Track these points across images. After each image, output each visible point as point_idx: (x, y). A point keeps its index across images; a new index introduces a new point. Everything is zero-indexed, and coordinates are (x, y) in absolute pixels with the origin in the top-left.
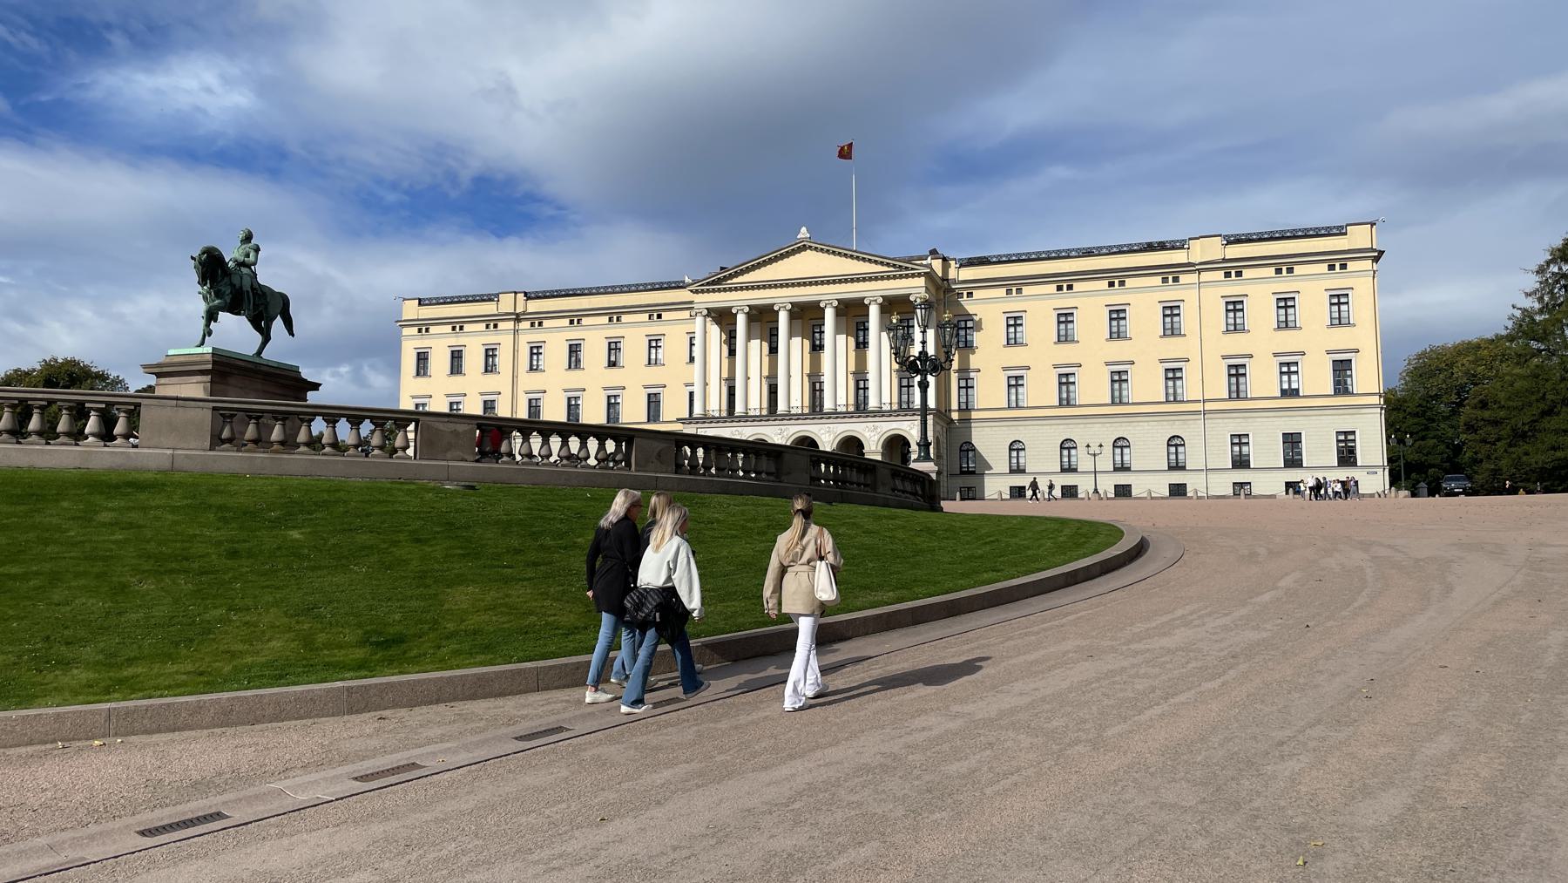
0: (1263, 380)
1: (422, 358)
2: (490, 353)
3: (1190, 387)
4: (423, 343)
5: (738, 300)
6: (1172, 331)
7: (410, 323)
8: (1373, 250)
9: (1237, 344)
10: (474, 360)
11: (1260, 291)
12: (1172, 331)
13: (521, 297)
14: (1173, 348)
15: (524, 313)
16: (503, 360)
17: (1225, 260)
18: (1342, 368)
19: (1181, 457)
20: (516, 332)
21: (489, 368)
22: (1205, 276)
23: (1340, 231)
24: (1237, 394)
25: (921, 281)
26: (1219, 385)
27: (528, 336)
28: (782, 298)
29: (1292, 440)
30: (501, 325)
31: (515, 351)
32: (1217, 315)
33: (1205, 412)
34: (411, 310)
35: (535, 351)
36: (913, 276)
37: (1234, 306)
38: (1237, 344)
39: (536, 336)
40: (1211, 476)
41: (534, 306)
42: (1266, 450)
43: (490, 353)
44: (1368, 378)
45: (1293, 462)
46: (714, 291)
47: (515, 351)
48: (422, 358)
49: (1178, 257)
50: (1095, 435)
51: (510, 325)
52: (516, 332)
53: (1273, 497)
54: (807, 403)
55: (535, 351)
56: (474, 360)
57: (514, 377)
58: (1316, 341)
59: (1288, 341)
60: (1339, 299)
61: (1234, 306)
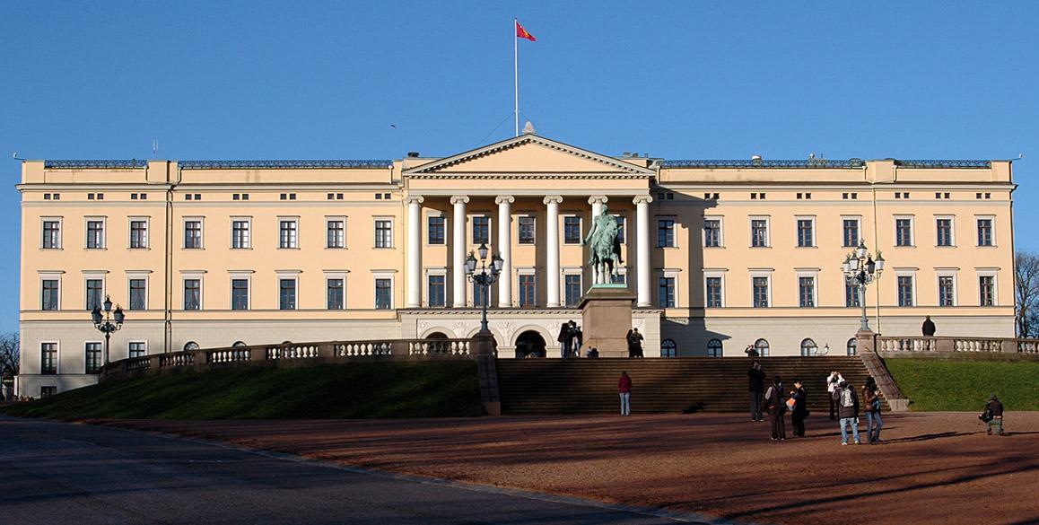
1: (49, 229)
4: (51, 210)
5: (458, 190)
7: (33, 185)
13: (174, 166)
15: (179, 184)
16: (154, 235)
17: (896, 182)
18: (986, 283)
20: (169, 204)
21: (135, 244)
22: (881, 195)
23: (986, 165)
27: (183, 211)
28: (504, 191)
30: (151, 196)
34: (32, 171)
35: (191, 227)
39: (193, 210)
41: (190, 176)
44: (1004, 292)
52: (169, 204)
54: (563, 298)
55: (191, 227)
59: (946, 256)
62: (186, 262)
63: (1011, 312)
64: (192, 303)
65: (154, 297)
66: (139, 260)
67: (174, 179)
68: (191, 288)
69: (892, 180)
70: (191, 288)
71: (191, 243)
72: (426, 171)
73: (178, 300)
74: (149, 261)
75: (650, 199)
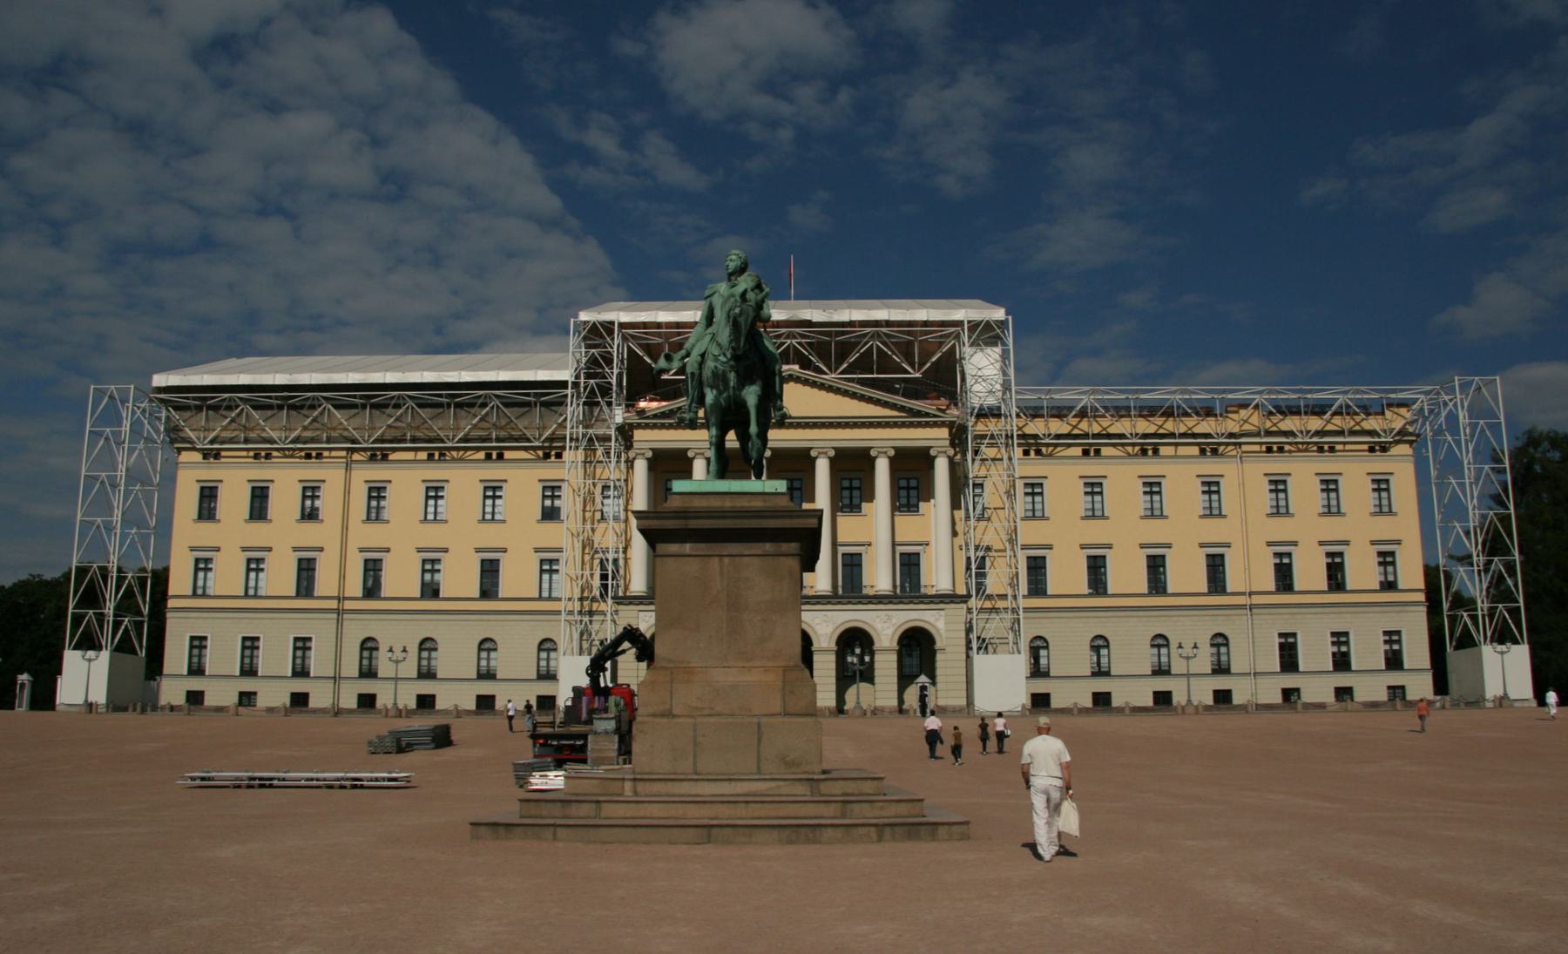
0: (1310, 572)
1: (208, 495)
2: (310, 491)
3: (1234, 578)
6: (1213, 512)
9: (1281, 529)
10: (286, 501)
11: (1303, 473)
12: (1213, 512)
14: (1214, 531)
16: (328, 503)
18: (1387, 559)
19: (1224, 658)
21: (310, 515)
25: (944, 433)
27: (365, 474)
29: (1340, 638)
31: (347, 492)
33: (1252, 607)
35: (376, 492)
36: (935, 425)
40: (1260, 680)
42: (1315, 652)
43: (310, 491)
45: (1342, 662)
46: (663, 426)
47: (347, 492)
48: (208, 495)
50: (1190, 633)
52: (348, 468)
53: (1321, 706)
55: (376, 492)
56: (286, 501)
57: (345, 527)
58: (1359, 530)
59: (1333, 529)
60: (1381, 485)
61: (1278, 485)
62: (367, 535)
63: (1421, 597)
64: (372, 590)
65: (325, 582)
66: (310, 534)
68: (373, 569)
70: (373, 569)
71: (374, 515)
72: (655, 416)
73: (355, 586)
75: (951, 452)
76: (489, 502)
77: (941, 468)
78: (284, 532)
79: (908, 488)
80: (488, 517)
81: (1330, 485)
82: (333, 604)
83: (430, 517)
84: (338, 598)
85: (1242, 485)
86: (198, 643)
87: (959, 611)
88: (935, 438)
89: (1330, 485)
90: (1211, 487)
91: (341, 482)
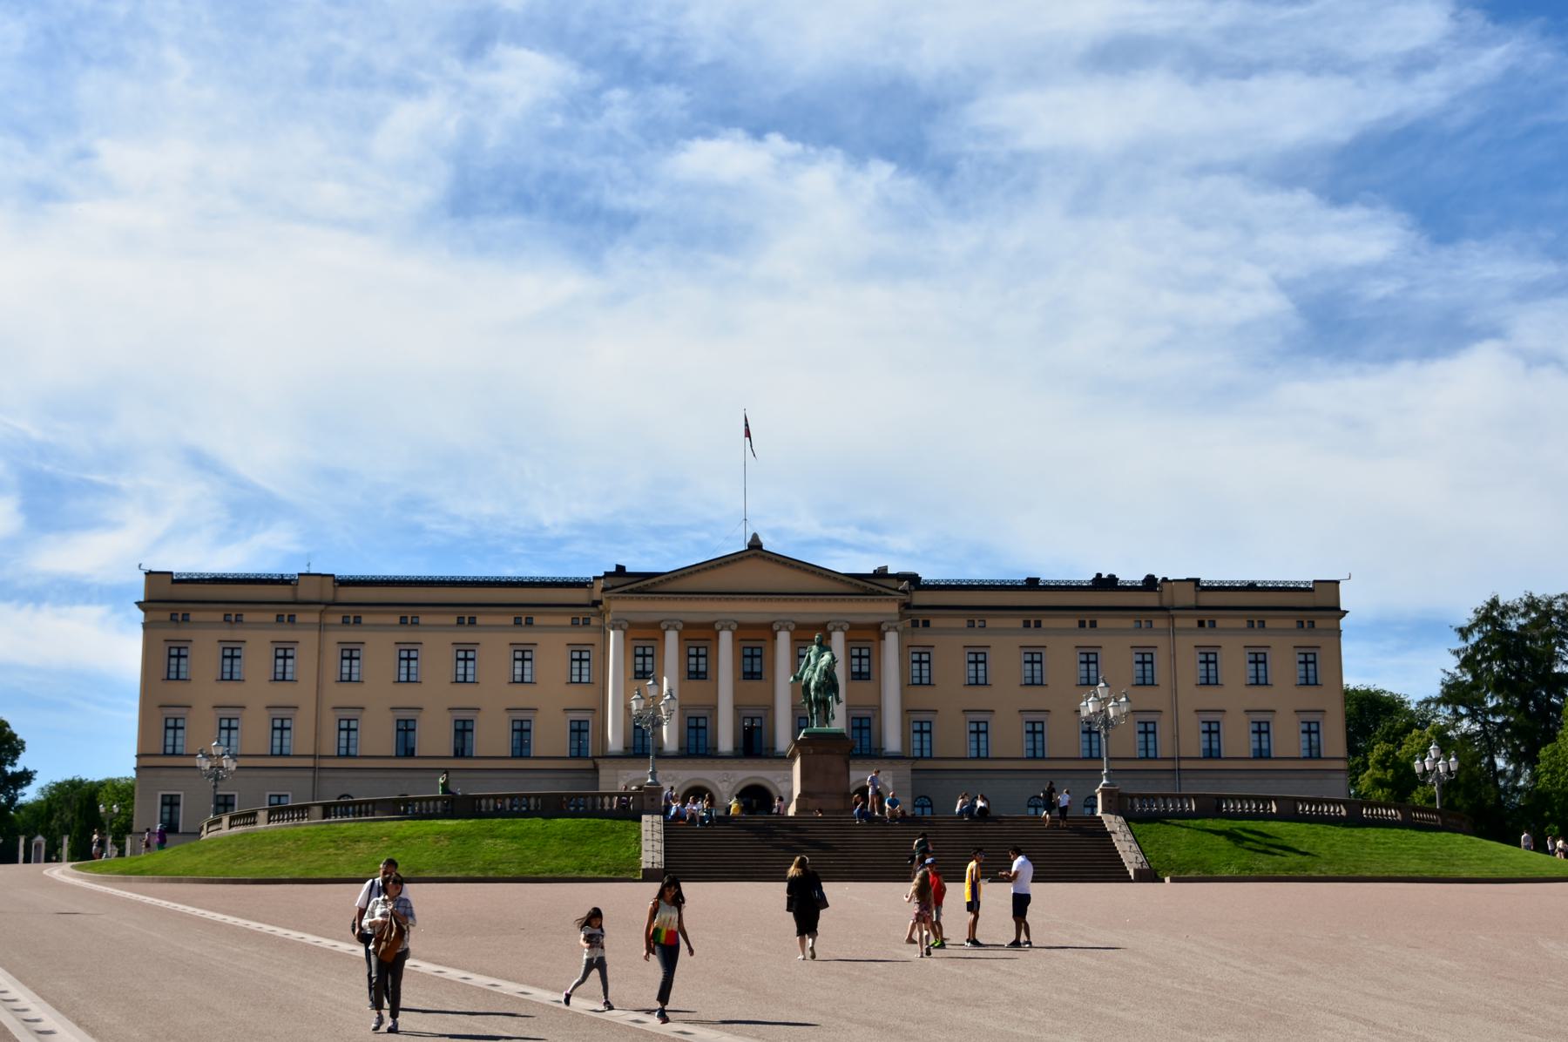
2: (284, 653)
8: (1338, 609)
9: (1210, 698)
16: (303, 664)
17: (1199, 608)
20: (322, 627)
22: (1179, 623)
24: (1211, 754)
26: (1193, 743)
32: (1190, 668)
37: (1209, 659)
38: (1210, 698)
39: (351, 635)
44: (1334, 740)
49: (1150, 599)
51: (315, 618)
52: (322, 627)
59: (1260, 698)
61: (1209, 659)
65: (301, 740)
66: (283, 693)
67: (329, 597)
69: (1191, 602)
74: (300, 693)
76: (461, 664)
77: (892, 639)
78: (256, 689)
79: (860, 657)
80: (461, 678)
81: (1258, 660)
82: (309, 762)
83: (403, 678)
84: (314, 756)
85: (1173, 657)
86: (171, 802)
87: (905, 769)
88: (887, 609)
89: (1258, 660)
90: (1145, 660)
91: (313, 647)
